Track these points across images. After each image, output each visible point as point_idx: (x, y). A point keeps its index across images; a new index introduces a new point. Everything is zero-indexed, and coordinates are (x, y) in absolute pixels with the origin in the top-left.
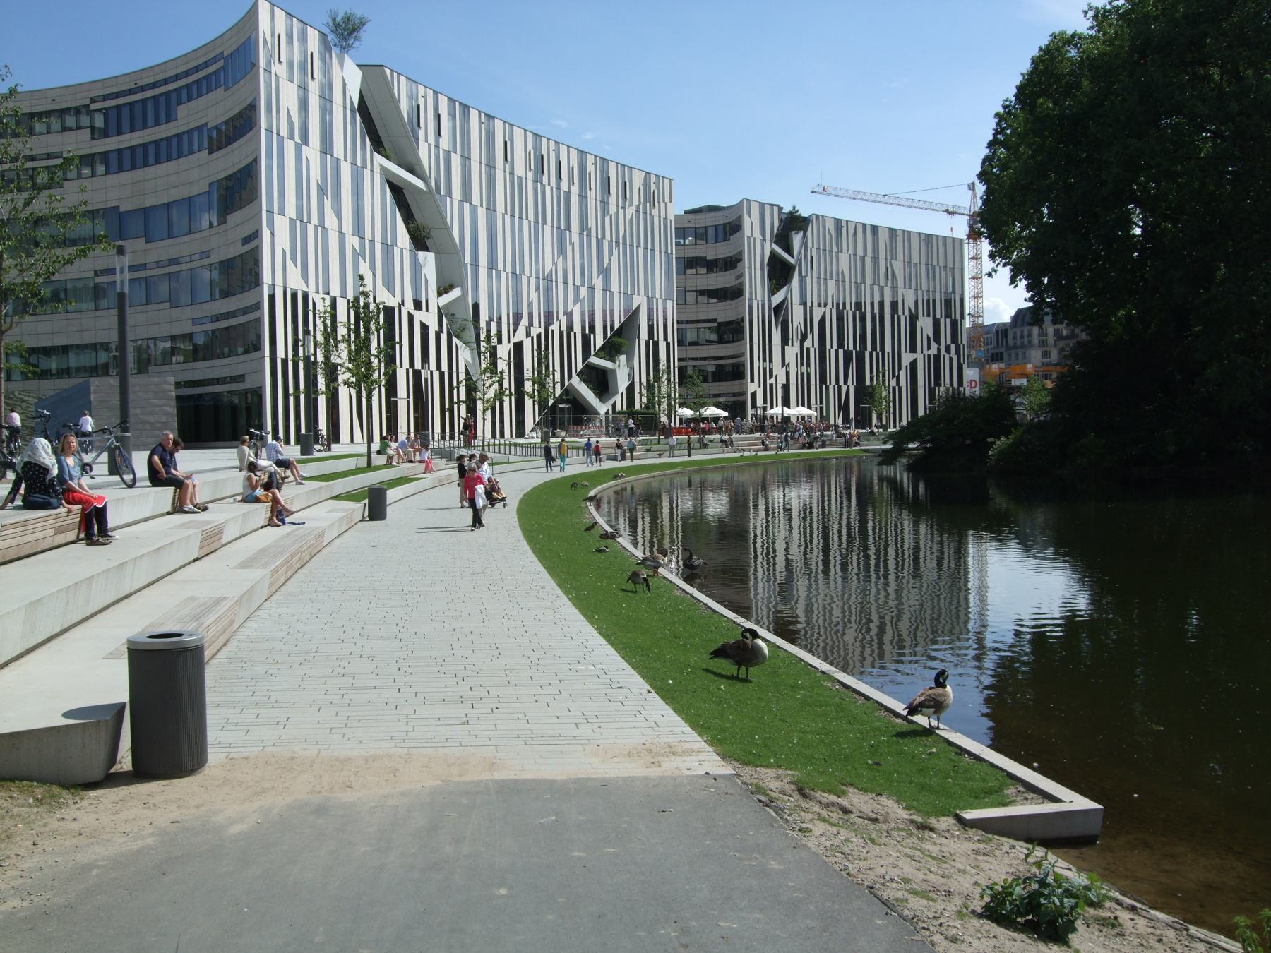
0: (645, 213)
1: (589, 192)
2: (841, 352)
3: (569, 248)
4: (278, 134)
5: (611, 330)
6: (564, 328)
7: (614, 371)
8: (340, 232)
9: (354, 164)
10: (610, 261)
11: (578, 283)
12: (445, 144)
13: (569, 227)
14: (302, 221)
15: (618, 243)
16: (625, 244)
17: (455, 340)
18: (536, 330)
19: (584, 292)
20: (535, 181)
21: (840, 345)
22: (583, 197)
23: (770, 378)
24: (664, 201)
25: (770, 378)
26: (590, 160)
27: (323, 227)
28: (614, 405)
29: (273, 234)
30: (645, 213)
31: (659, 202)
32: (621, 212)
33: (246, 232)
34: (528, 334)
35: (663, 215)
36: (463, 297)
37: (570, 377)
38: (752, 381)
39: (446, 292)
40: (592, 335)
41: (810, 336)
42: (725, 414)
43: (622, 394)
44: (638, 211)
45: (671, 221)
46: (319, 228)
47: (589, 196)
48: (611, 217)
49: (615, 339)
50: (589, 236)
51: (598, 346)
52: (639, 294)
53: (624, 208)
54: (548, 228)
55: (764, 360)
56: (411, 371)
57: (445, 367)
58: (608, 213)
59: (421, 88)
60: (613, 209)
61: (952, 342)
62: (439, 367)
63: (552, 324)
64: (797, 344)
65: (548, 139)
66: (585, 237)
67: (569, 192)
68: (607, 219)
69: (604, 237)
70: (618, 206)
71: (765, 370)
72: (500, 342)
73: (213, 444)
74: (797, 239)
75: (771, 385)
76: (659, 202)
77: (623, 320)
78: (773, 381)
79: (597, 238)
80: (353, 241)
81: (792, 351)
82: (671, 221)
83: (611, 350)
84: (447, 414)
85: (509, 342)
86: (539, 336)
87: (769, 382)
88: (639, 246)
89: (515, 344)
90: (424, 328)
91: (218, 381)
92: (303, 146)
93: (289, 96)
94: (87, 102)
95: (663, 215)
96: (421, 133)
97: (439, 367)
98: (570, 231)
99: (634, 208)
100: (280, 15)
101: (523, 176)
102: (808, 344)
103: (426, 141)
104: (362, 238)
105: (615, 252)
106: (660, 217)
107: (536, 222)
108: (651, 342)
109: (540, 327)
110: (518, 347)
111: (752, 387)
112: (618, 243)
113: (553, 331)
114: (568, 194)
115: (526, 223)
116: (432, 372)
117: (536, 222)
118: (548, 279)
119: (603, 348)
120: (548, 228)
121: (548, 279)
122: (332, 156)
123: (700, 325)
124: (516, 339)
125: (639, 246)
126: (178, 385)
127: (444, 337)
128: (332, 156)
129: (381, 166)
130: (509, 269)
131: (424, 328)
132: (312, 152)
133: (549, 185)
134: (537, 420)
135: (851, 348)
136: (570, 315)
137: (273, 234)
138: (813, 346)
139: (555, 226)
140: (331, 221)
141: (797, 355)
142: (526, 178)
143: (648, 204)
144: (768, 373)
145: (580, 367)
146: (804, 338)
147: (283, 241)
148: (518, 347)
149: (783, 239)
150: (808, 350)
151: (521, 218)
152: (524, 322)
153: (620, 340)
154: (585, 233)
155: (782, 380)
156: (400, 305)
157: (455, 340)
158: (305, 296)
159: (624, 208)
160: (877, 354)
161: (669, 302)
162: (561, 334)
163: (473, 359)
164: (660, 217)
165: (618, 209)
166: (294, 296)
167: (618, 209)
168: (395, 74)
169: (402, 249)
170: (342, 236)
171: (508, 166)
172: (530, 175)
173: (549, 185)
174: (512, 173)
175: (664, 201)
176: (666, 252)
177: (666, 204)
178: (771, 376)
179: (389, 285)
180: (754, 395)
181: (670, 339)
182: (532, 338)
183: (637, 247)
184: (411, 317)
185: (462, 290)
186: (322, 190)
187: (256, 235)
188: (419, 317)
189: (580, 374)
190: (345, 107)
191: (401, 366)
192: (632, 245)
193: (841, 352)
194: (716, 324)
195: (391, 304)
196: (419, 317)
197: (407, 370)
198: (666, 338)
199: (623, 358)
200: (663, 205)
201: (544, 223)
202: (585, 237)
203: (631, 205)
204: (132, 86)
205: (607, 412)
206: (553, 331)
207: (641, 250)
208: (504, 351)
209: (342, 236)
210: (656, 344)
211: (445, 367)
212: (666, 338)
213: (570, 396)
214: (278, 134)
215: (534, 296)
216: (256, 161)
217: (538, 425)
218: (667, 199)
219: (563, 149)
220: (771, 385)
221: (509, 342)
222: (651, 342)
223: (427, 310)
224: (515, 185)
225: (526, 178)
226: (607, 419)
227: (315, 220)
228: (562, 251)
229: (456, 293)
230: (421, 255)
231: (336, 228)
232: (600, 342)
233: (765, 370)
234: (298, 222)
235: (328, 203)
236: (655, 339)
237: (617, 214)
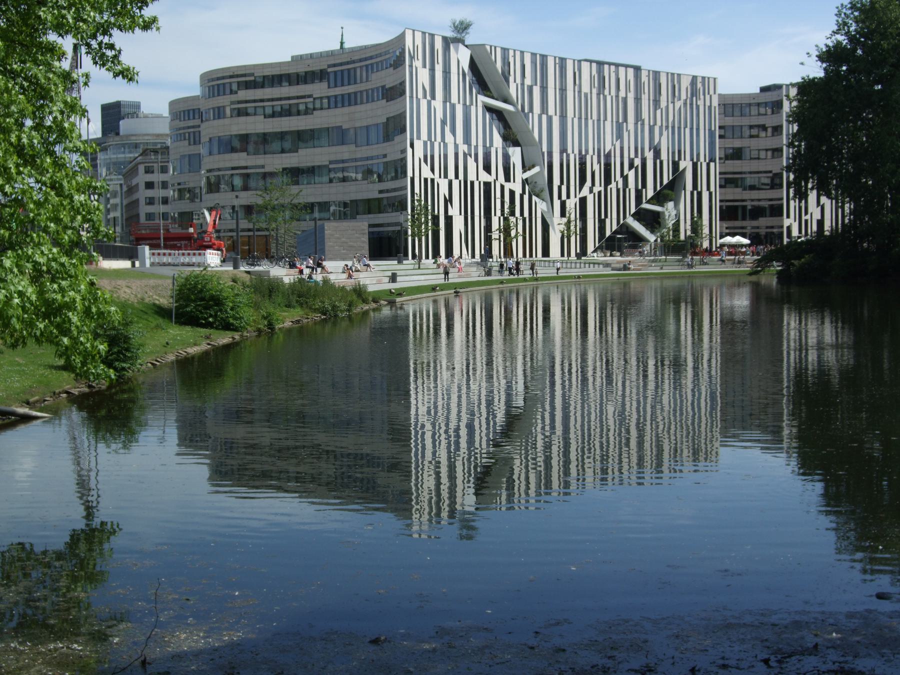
0: (691, 104)
1: (643, 95)
3: (626, 134)
5: (660, 186)
6: (620, 186)
7: (663, 213)
10: (660, 139)
11: (632, 156)
12: (528, 81)
13: (625, 119)
14: (431, 141)
15: (667, 127)
16: (673, 127)
17: (534, 198)
18: (596, 189)
19: (638, 162)
20: (598, 94)
22: (638, 100)
24: (709, 94)
26: (644, 74)
30: (691, 104)
32: (671, 106)
34: (591, 191)
35: (708, 104)
36: (540, 173)
37: (625, 217)
38: (788, 217)
39: (529, 169)
40: (644, 190)
42: (746, 241)
44: (685, 104)
45: (715, 107)
47: (643, 97)
48: (662, 109)
49: (666, 191)
50: (643, 124)
51: (649, 197)
52: (685, 160)
54: (608, 124)
56: (502, 218)
57: (526, 214)
58: (659, 108)
60: (663, 104)
62: (522, 214)
63: (610, 183)
67: (626, 98)
68: (659, 112)
69: (655, 124)
70: (668, 101)
72: (568, 197)
73: (391, 258)
75: (806, 221)
77: (671, 178)
78: (808, 217)
79: (649, 124)
80: (463, 148)
82: (715, 107)
83: (660, 198)
84: (566, 240)
85: (576, 197)
86: (600, 193)
87: (804, 218)
88: (686, 127)
90: (512, 193)
91: (389, 225)
94: (326, 67)
95: (708, 104)
96: (511, 79)
97: (522, 214)
99: (682, 101)
101: (589, 92)
103: (515, 81)
104: (469, 145)
105: (665, 133)
106: (705, 105)
107: (599, 120)
109: (600, 186)
110: (583, 201)
111: (787, 222)
112: (667, 127)
113: (611, 189)
114: (625, 100)
115: (590, 122)
117: (599, 120)
118: (608, 156)
119: (652, 198)
120: (608, 124)
121: (608, 156)
122: (450, 102)
123: (760, 175)
124: (582, 195)
125: (686, 127)
126: (370, 226)
127: (526, 197)
129: (483, 102)
130: (576, 151)
131: (512, 193)
133: (610, 94)
134: (597, 245)
136: (625, 179)
139: (614, 120)
140: (449, 138)
142: (591, 93)
143: (694, 98)
145: (633, 210)
148: (583, 201)
151: (586, 119)
152: (589, 183)
153: (670, 192)
155: (817, 215)
156: (495, 181)
157: (534, 198)
158: (433, 180)
159: (673, 102)
161: (712, 164)
162: (618, 190)
163: (548, 209)
164: (705, 105)
166: (426, 180)
169: (497, 149)
170: (456, 146)
171: (576, 87)
172: (595, 91)
173: (610, 94)
174: (580, 92)
175: (709, 94)
176: (710, 130)
177: (711, 96)
178: (806, 213)
179: (487, 169)
180: (789, 228)
181: (712, 189)
183: (684, 128)
184: (502, 187)
185: (541, 168)
186: (444, 123)
187: (404, 151)
188: (508, 186)
189: (633, 216)
191: (495, 215)
192: (679, 128)
195: (489, 180)
196: (508, 186)
197: (500, 218)
198: (708, 188)
199: (671, 205)
200: (708, 97)
201: (605, 119)
203: (680, 99)
204: (349, 60)
205: (656, 241)
206: (611, 189)
207: (688, 131)
208: (572, 203)
209: (456, 146)
210: (700, 194)
211: (526, 214)
212: (708, 188)
213: (624, 229)
215: (596, 167)
217: (599, 248)
218: (712, 92)
221: (576, 197)
222: (695, 192)
223: (514, 182)
224: (583, 100)
225: (591, 93)
226: (656, 245)
227: (439, 139)
228: (620, 136)
229: (536, 169)
231: (453, 141)
232: (650, 193)
236: (699, 190)
237: (667, 107)
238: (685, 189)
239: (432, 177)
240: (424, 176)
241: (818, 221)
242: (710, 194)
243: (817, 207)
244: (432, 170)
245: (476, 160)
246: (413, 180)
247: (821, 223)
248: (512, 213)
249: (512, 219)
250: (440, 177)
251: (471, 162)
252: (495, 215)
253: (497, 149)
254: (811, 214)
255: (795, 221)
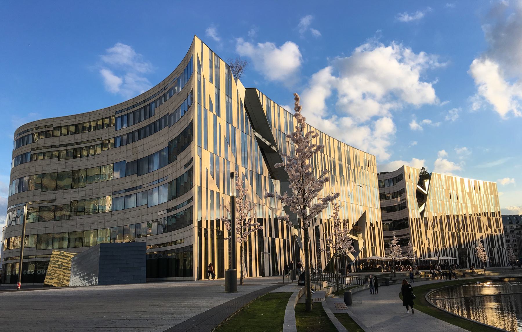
2: (450, 233)
4: (204, 107)
8: (236, 164)
9: (242, 131)
21: (450, 229)
23: (422, 245)
25: (422, 245)
27: (227, 160)
28: (359, 257)
29: (201, 159)
31: (370, 165)
32: (356, 169)
33: (187, 161)
38: (415, 246)
41: (436, 225)
43: (362, 251)
46: (226, 160)
50: (344, 178)
53: (357, 167)
55: (419, 237)
56: (270, 238)
59: (272, 102)
61: (497, 228)
64: (431, 228)
65: (325, 134)
66: (342, 179)
71: (419, 241)
74: (426, 182)
75: (423, 248)
76: (370, 165)
78: (423, 246)
81: (430, 232)
85: (313, 226)
86: (325, 223)
87: (422, 246)
89: (315, 227)
92: (217, 117)
93: (210, 89)
98: (336, 176)
100: (206, 49)
102: (436, 229)
108: (372, 227)
113: (331, 221)
116: (280, 239)
128: (232, 125)
132: (222, 120)
133: (327, 154)
135: (454, 231)
137: (201, 159)
138: (438, 230)
141: (432, 234)
143: (366, 166)
144: (421, 243)
146: (434, 226)
147: (206, 163)
149: (421, 183)
150: (436, 232)
154: (342, 177)
159: (357, 167)
160: (465, 234)
165: (354, 167)
167: (354, 167)
168: (261, 93)
169: (265, 177)
175: (372, 165)
180: (416, 252)
181: (379, 227)
182: (323, 224)
186: (227, 142)
190: (238, 103)
193: (450, 233)
194: (392, 222)
198: (377, 226)
202: (342, 179)
203: (359, 166)
206: (331, 221)
210: (374, 229)
212: (377, 226)
214: (204, 107)
216: (191, 125)
219: (331, 139)
220: (423, 248)
221: (313, 226)
230: (274, 181)
233: (419, 241)
234: (215, 155)
235: (230, 149)
236: (373, 226)
238: (367, 225)
239: (218, 191)
240: (210, 188)
241: (428, 248)
242: (379, 229)
243: (426, 240)
244: (218, 184)
245: (251, 184)
246: (200, 188)
247: (429, 249)
248: (277, 236)
249: (277, 241)
250: (224, 193)
251: (248, 182)
252: (266, 236)
253: (265, 177)
254: (424, 244)
255: (418, 248)
